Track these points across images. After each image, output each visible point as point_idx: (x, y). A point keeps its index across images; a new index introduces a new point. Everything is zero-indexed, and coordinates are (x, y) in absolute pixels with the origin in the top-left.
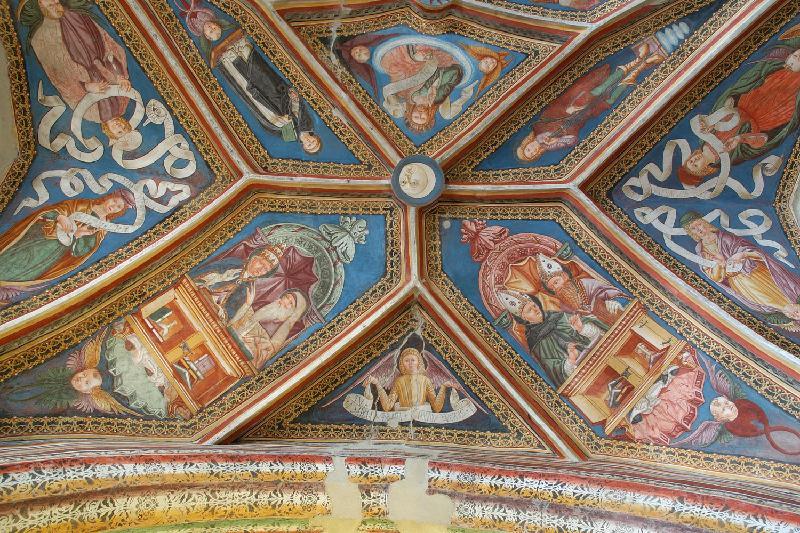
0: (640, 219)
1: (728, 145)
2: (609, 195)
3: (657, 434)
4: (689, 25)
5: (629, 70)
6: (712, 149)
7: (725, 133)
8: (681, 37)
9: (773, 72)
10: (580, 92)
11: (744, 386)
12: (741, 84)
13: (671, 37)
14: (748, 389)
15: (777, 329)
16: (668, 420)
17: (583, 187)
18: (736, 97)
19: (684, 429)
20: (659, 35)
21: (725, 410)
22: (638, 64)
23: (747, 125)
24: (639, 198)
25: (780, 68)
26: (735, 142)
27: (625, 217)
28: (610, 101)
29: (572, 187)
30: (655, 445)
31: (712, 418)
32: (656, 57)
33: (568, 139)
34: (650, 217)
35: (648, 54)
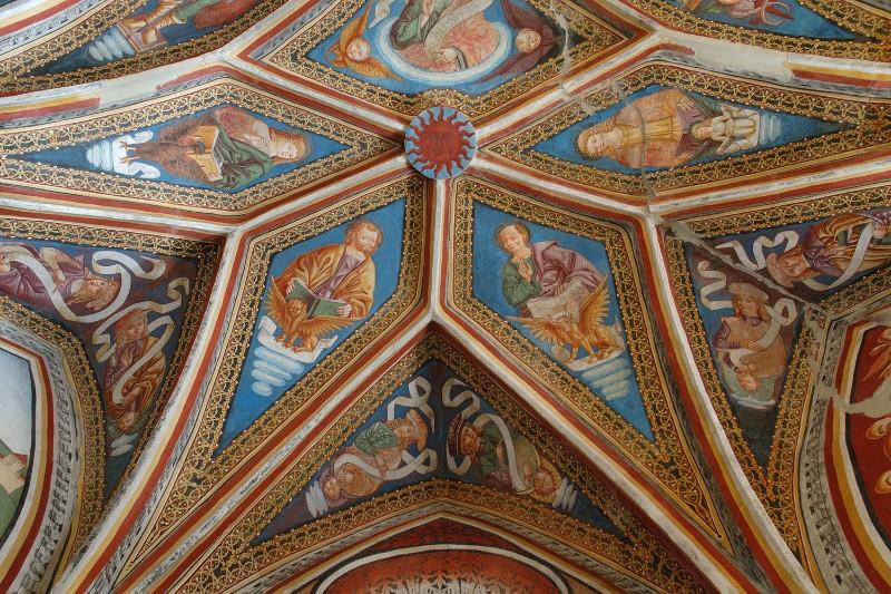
4: (89, 55)
8: (99, 44)
20: (130, 51)
22: (156, 22)
35: (144, 31)
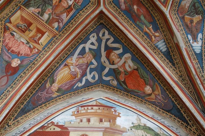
0: (93, 34)
1: (121, 67)
2: (101, 24)
3: (7, 41)
4: (165, 52)
5: (149, 29)
6: (119, 62)
7: (125, 66)
8: (161, 49)
9: (145, 81)
10: (143, 10)
11: (24, 69)
12: (142, 71)
13: (162, 46)
14: (23, 70)
15: (47, 81)
16: (12, 45)
17: (102, 12)
18: (137, 70)
19: (9, 50)
20: (163, 40)
21: (15, 63)
22: (152, 33)
23: (127, 74)
24: (101, 35)
25: (146, 84)
26: (122, 70)
27: (92, 30)
28: (138, 23)
29: (102, 8)
30: (3, 40)
31: (12, 59)
32: (154, 39)
33: (123, 7)
34: (93, 39)
35: (155, 36)
